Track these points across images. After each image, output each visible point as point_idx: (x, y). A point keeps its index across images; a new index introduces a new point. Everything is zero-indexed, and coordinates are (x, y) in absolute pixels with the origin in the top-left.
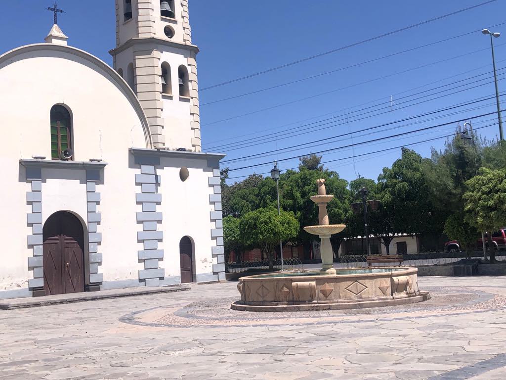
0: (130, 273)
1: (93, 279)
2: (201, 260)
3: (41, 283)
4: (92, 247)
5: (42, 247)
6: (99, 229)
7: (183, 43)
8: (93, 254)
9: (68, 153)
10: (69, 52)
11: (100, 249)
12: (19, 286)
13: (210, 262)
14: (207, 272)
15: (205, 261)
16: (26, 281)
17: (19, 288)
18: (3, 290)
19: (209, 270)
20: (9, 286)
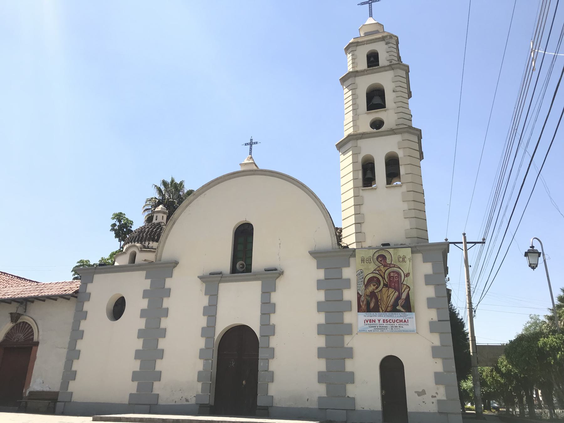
0: (308, 400)
1: (261, 401)
2: (416, 392)
3: (208, 399)
4: (262, 365)
5: (210, 361)
6: (274, 342)
7: (395, 127)
8: (262, 372)
9: (241, 266)
10: (254, 174)
11: (273, 366)
12: (187, 400)
13: (433, 397)
14: (426, 410)
15: (423, 393)
16: (195, 396)
17: (187, 403)
18: (174, 403)
19: (431, 407)
20: (180, 399)
